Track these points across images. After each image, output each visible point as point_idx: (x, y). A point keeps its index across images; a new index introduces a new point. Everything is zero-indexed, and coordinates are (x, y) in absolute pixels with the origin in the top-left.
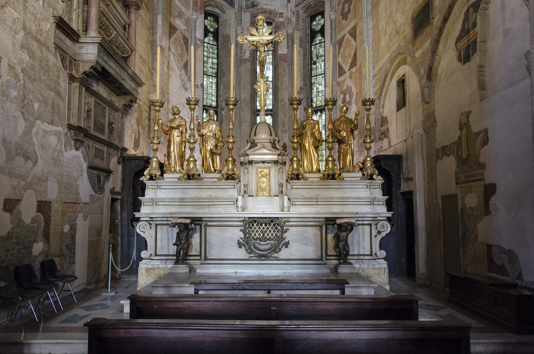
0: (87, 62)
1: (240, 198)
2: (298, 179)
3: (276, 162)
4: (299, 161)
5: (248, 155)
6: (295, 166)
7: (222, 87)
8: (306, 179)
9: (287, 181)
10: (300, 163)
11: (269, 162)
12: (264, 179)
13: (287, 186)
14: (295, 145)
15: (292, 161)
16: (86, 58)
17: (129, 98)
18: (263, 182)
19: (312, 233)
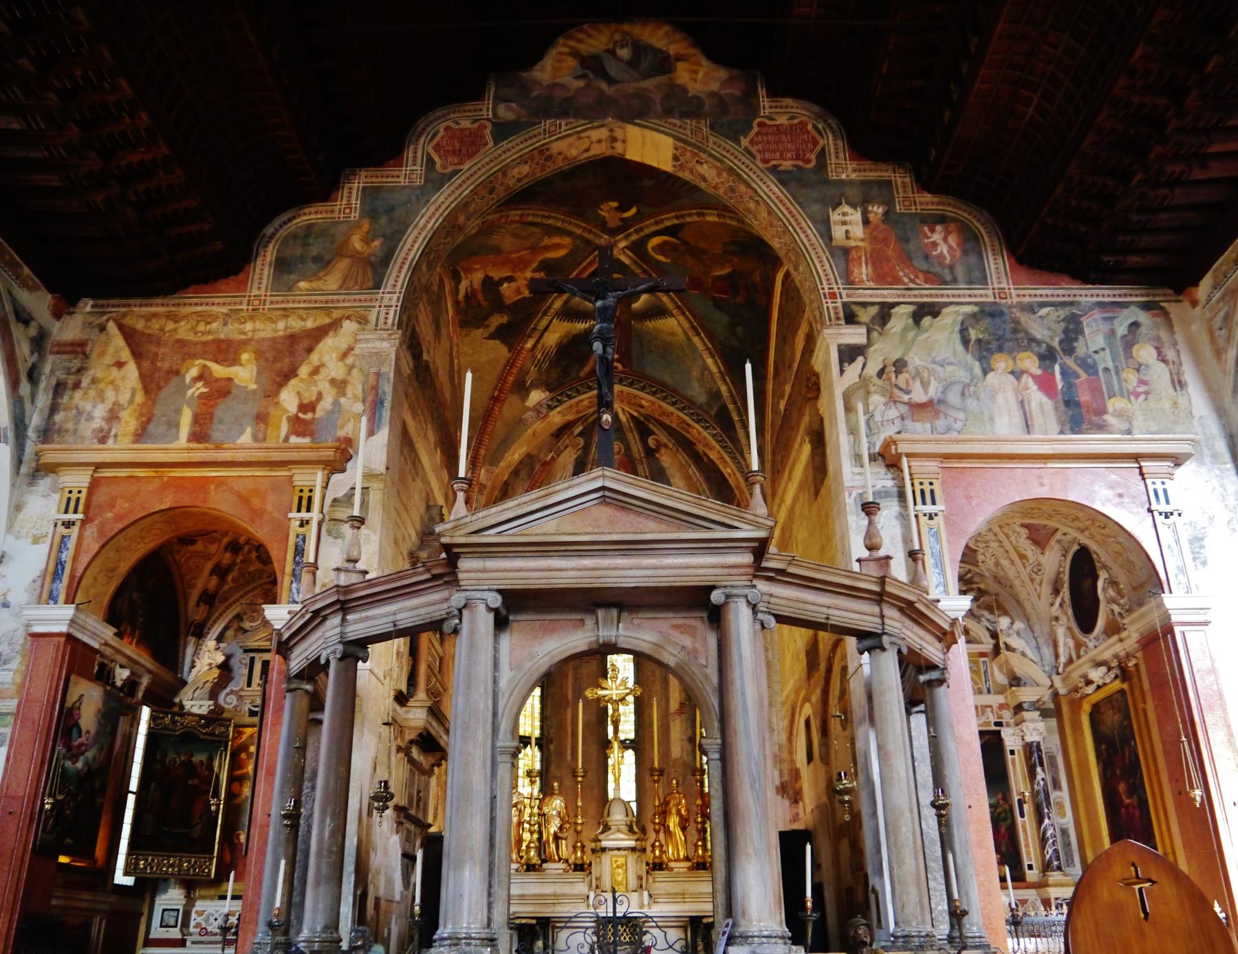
0: (414, 728)
1: (592, 895)
2: (661, 869)
3: (633, 849)
4: (661, 846)
5: (600, 841)
6: (657, 853)
7: (549, 702)
8: (671, 869)
9: (647, 872)
10: (664, 849)
11: (625, 849)
12: (620, 871)
13: (647, 879)
14: (657, 827)
15: (653, 846)
16: (413, 724)
17: (439, 755)
18: (619, 874)
19: (674, 935)
